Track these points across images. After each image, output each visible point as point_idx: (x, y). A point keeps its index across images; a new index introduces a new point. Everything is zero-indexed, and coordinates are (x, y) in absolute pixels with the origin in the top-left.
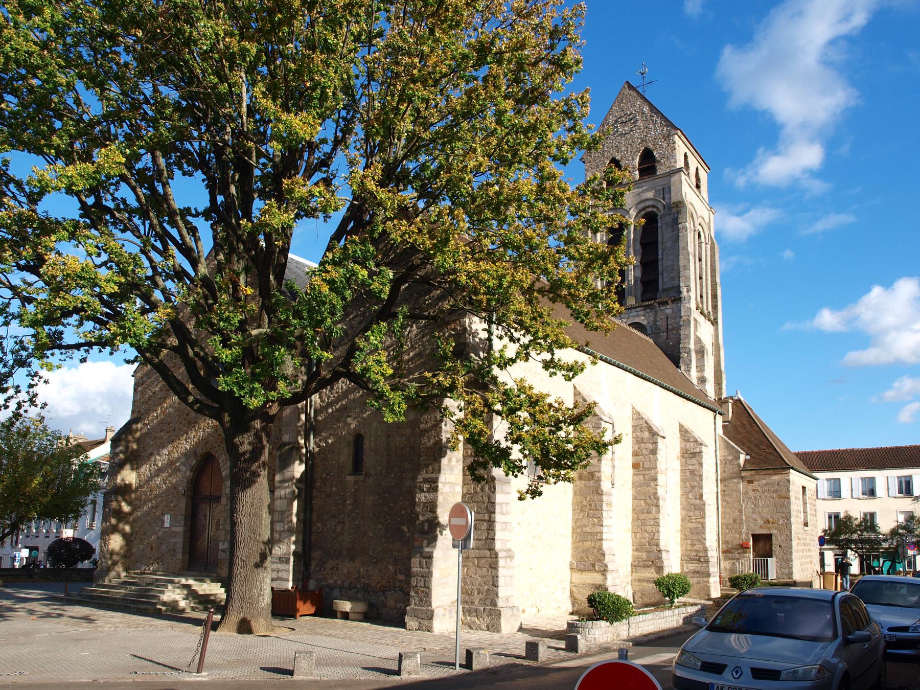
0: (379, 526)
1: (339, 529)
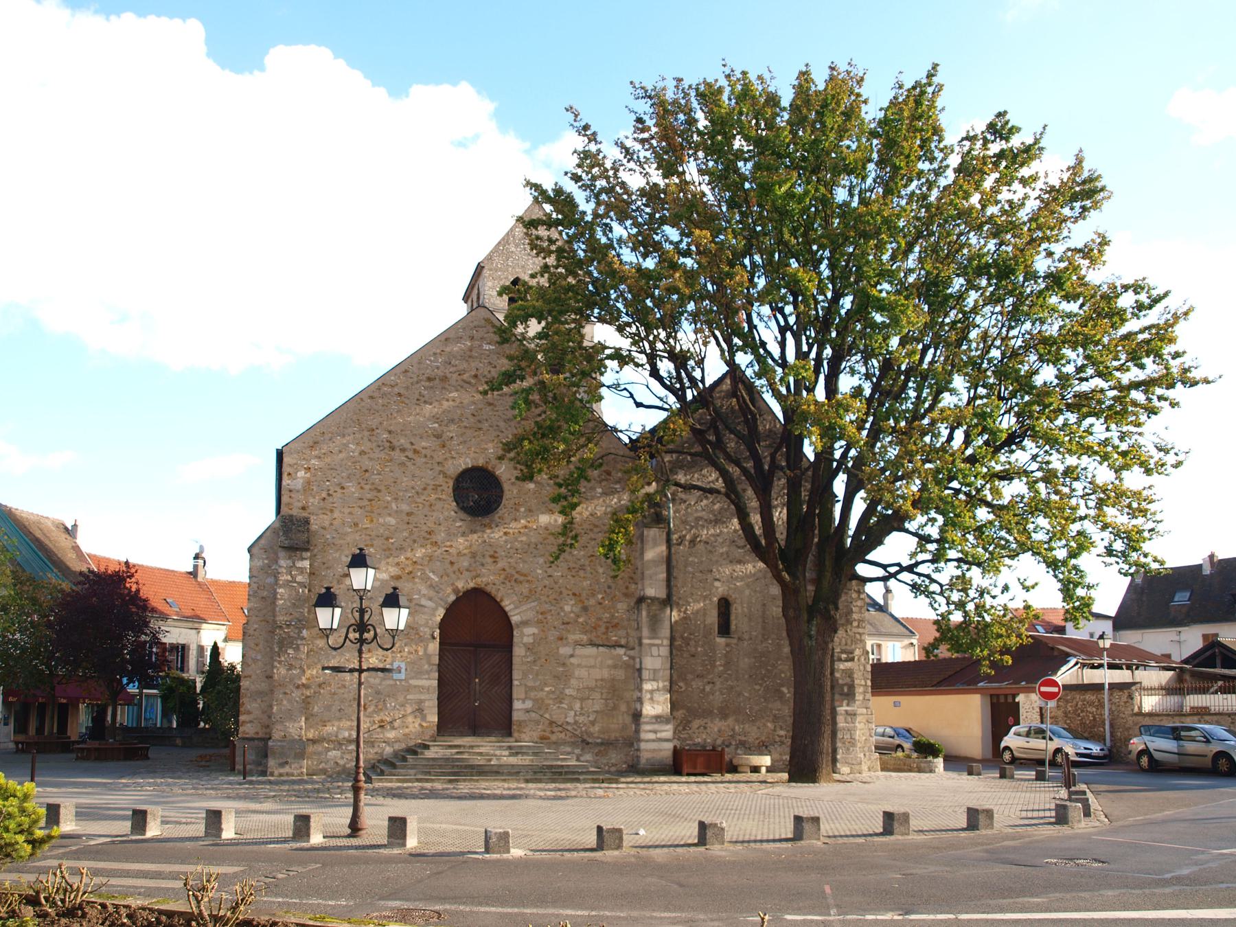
0: (757, 687)
1: (708, 688)
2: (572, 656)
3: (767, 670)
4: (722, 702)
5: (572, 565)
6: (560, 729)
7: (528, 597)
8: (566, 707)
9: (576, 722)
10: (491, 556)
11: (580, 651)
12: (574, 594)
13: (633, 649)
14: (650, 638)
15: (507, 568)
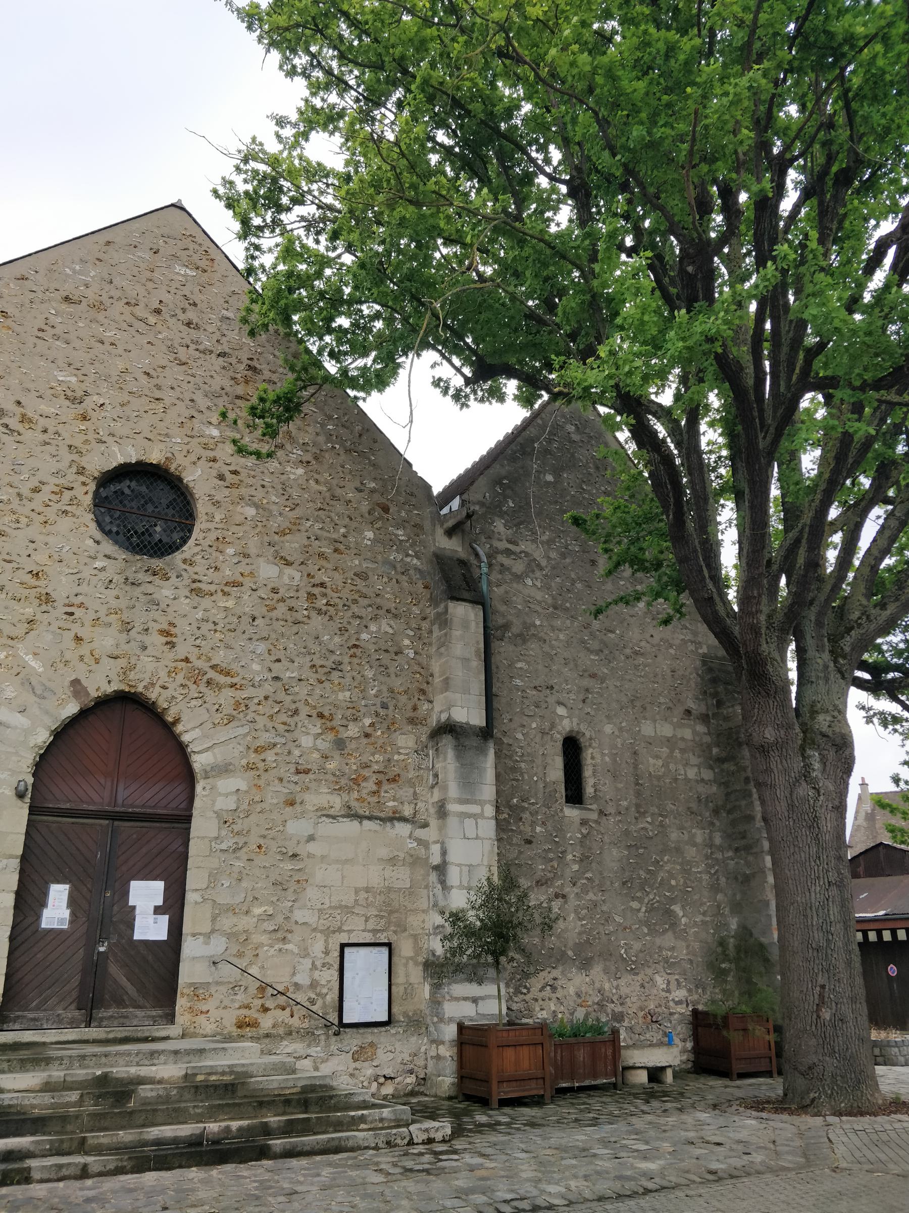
0: (635, 905)
1: (556, 905)
2: (311, 838)
3: (649, 872)
4: (580, 934)
5: (319, 662)
6: (282, 1000)
7: (231, 719)
8: (296, 951)
9: (314, 985)
10: (163, 632)
11: (327, 828)
12: (321, 716)
13: (425, 825)
14: (462, 801)
15: (192, 658)
